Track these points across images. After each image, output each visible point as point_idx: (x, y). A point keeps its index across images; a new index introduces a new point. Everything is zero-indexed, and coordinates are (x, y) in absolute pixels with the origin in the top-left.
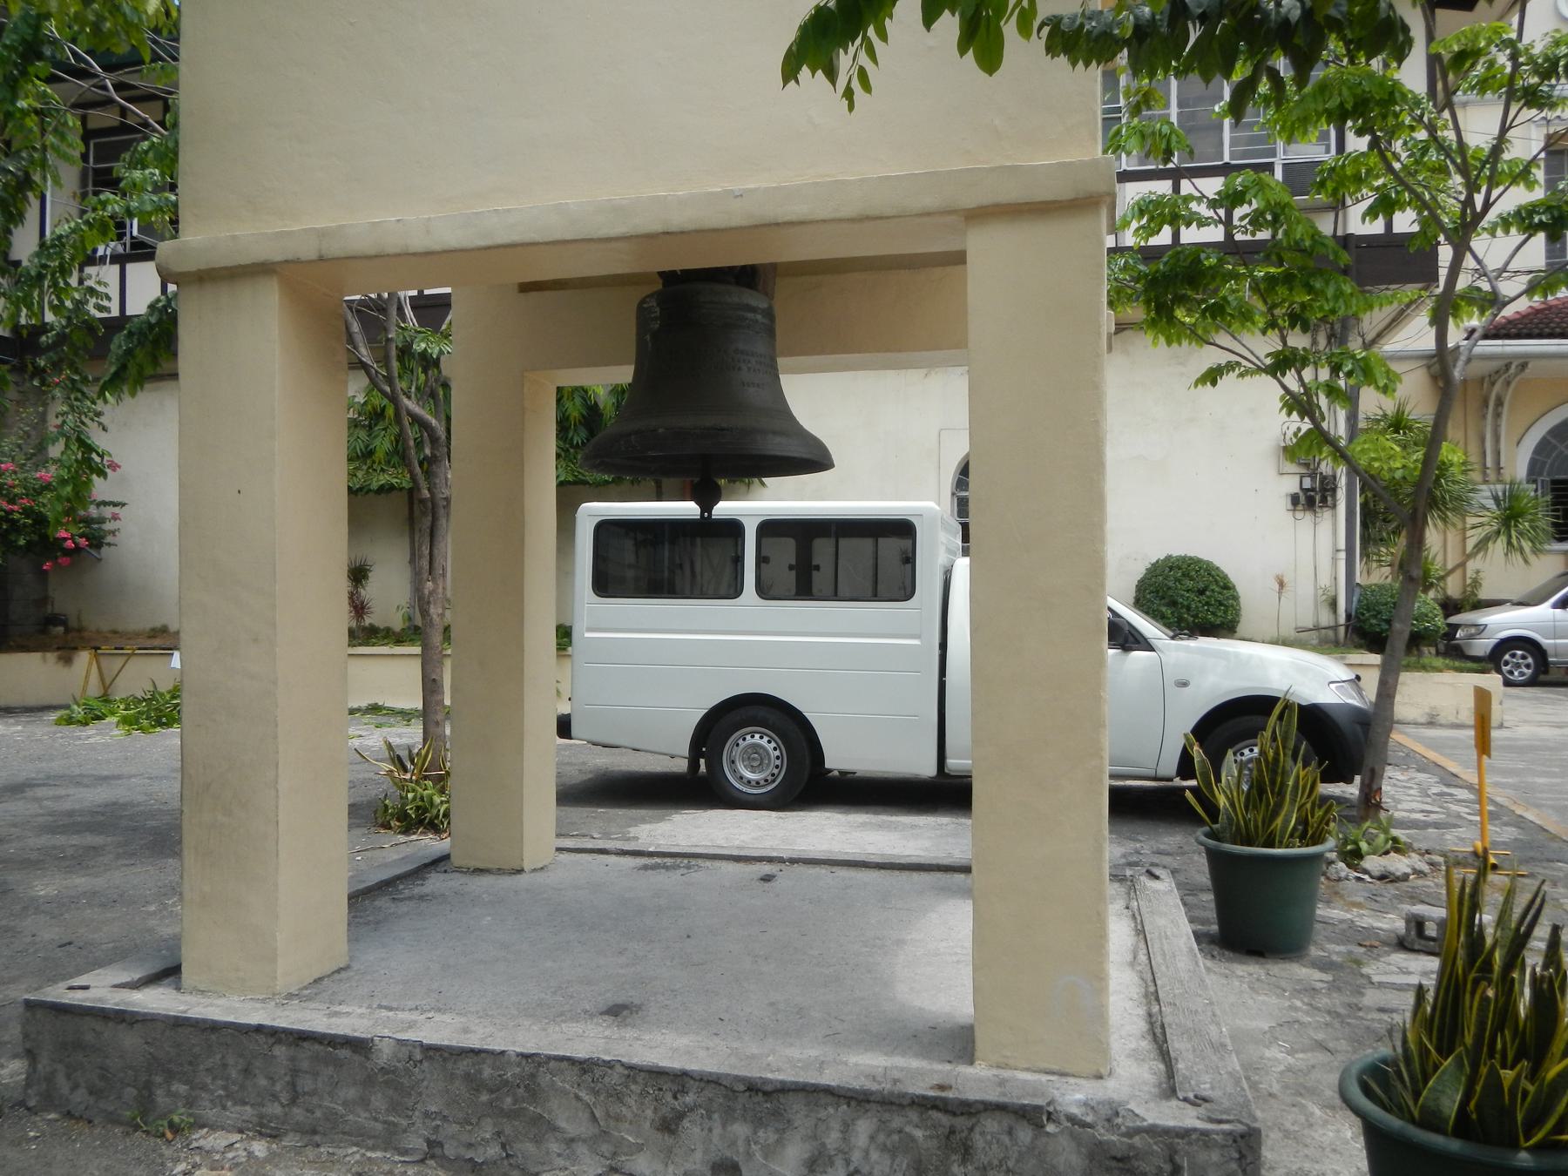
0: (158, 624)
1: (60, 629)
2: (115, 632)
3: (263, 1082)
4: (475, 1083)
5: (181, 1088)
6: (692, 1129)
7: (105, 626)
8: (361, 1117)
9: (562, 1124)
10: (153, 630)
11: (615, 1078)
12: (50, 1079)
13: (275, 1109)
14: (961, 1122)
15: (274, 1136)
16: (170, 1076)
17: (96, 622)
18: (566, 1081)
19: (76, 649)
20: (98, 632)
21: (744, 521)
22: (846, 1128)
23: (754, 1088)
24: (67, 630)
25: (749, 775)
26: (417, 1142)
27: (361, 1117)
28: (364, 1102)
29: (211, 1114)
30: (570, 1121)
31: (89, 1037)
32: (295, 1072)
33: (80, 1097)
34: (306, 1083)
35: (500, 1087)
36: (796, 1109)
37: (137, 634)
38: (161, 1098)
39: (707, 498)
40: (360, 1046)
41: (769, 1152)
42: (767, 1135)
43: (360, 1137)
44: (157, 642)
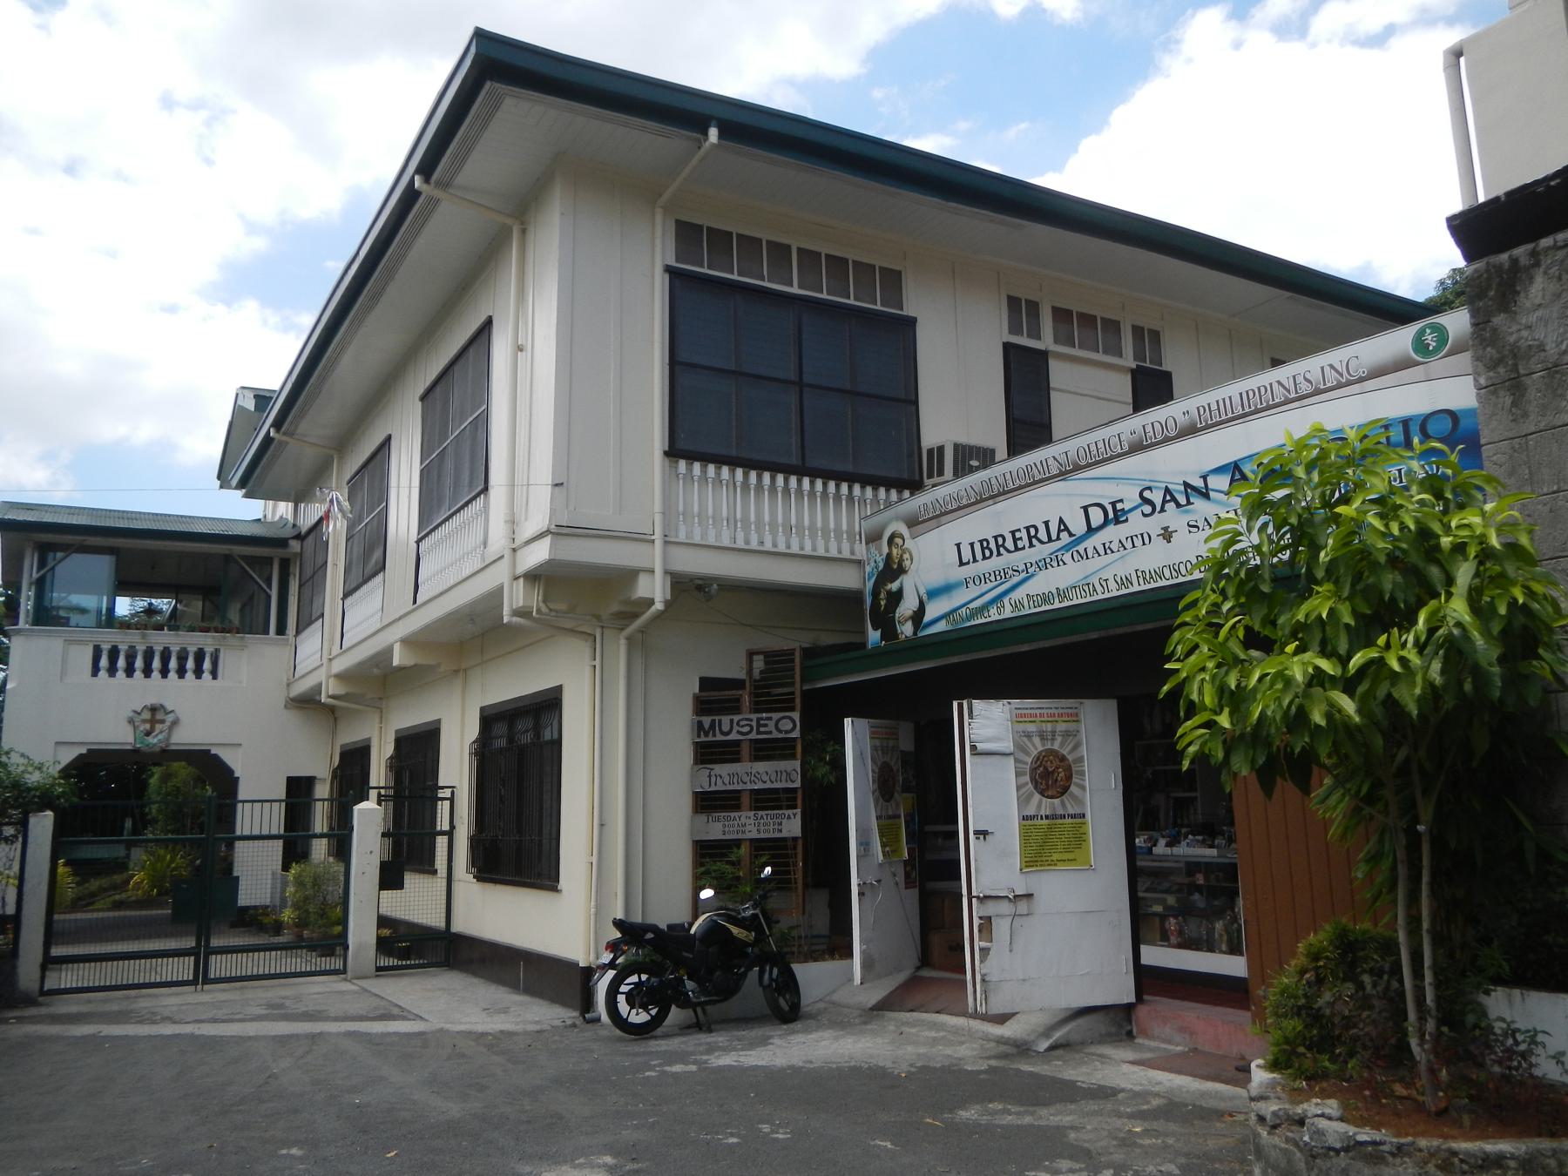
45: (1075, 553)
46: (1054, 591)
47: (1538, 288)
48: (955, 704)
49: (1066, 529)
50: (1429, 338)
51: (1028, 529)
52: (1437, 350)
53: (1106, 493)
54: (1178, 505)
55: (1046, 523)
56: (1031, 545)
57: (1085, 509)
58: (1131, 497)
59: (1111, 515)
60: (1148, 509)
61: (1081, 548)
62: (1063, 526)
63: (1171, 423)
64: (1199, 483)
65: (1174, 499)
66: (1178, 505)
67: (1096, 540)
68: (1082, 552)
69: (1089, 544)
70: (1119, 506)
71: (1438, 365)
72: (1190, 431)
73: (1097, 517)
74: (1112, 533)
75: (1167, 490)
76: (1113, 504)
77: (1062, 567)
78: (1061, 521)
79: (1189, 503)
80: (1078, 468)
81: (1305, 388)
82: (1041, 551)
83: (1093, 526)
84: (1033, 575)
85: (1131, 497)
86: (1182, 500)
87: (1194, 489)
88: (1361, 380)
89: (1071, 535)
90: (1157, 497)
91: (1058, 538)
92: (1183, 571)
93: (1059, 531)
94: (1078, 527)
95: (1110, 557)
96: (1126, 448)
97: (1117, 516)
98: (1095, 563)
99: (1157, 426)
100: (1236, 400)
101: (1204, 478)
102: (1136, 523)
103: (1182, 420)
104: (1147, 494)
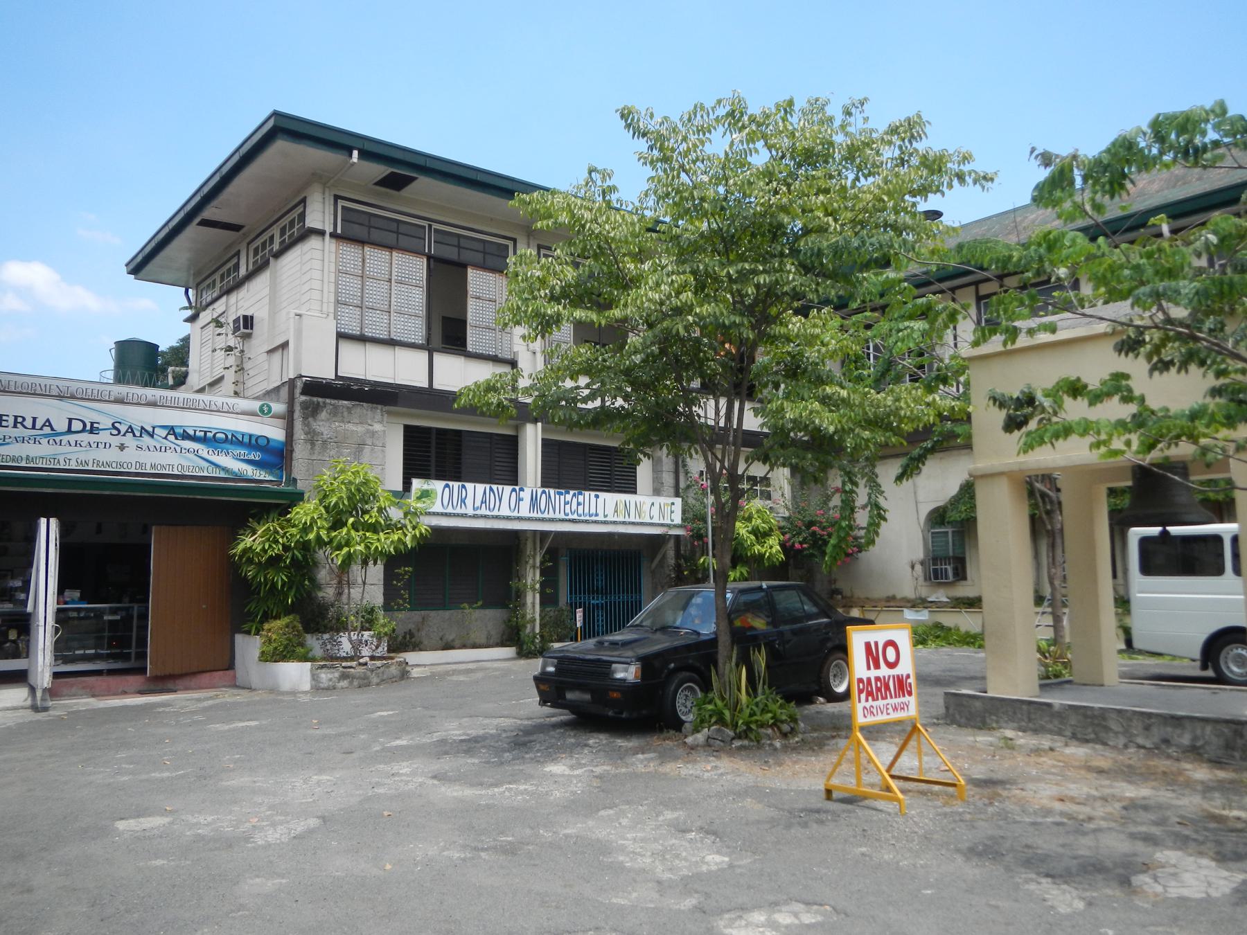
0: (890, 594)
1: (840, 597)
2: (868, 599)
3: (1020, 716)
4: (1086, 716)
5: (994, 718)
6: (1155, 730)
7: (862, 596)
8: (1050, 726)
9: (1113, 727)
10: (888, 597)
11: (1128, 714)
12: (953, 715)
13: (1023, 724)
14: (1239, 727)
15: (1024, 731)
16: (991, 714)
17: (859, 593)
18: (1114, 716)
19: (852, 607)
20: (859, 598)
21: (1223, 535)
22: (1203, 729)
23: (1173, 717)
24: (843, 598)
25: (1235, 669)
26: (1068, 733)
27: (1050, 726)
28: (1051, 722)
29: (1004, 725)
30: (1114, 726)
31: (965, 703)
32: (1029, 713)
33: (963, 721)
34: (1033, 716)
35: (1093, 717)
36: (1187, 724)
37: (880, 600)
38: (988, 721)
39: (1165, 533)
40: (1049, 705)
41: (1180, 736)
42: (1178, 731)
43: (1051, 732)
44: (892, 604)
45: (51, 442)
46: (24, 456)
47: (324, 415)
48: (43, 521)
49: (50, 425)
50: (265, 409)
51: (16, 417)
52: (267, 414)
53: (89, 417)
54: (134, 435)
55: (34, 419)
56: (15, 426)
57: (70, 420)
58: (106, 422)
59: (88, 427)
60: (115, 432)
61: (58, 439)
62: (48, 423)
63: (144, 397)
64: (150, 430)
65: (132, 432)
66: (134, 435)
67: (72, 438)
68: (58, 441)
69: (65, 438)
70: (95, 425)
71: (266, 419)
72: (153, 404)
73: (77, 426)
74: (85, 437)
75: (130, 427)
76: (92, 424)
77: (37, 445)
78: (48, 420)
79: (141, 436)
80: (73, 397)
81: (213, 407)
82: (20, 431)
83: (73, 429)
84: (8, 444)
85: (106, 422)
86: (138, 434)
87: (146, 431)
88: (237, 413)
89: (52, 429)
90: (123, 429)
91: (41, 429)
92: (125, 466)
93: (44, 425)
94: (61, 426)
95: (78, 448)
96: (112, 399)
97: (93, 430)
98: (68, 449)
99: (135, 396)
100: (181, 400)
101: (154, 428)
102: (104, 437)
103: (150, 398)
104: (117, 425)
